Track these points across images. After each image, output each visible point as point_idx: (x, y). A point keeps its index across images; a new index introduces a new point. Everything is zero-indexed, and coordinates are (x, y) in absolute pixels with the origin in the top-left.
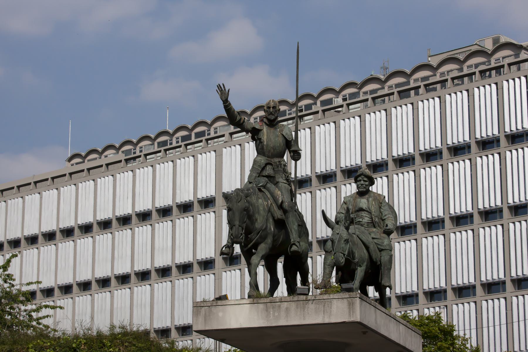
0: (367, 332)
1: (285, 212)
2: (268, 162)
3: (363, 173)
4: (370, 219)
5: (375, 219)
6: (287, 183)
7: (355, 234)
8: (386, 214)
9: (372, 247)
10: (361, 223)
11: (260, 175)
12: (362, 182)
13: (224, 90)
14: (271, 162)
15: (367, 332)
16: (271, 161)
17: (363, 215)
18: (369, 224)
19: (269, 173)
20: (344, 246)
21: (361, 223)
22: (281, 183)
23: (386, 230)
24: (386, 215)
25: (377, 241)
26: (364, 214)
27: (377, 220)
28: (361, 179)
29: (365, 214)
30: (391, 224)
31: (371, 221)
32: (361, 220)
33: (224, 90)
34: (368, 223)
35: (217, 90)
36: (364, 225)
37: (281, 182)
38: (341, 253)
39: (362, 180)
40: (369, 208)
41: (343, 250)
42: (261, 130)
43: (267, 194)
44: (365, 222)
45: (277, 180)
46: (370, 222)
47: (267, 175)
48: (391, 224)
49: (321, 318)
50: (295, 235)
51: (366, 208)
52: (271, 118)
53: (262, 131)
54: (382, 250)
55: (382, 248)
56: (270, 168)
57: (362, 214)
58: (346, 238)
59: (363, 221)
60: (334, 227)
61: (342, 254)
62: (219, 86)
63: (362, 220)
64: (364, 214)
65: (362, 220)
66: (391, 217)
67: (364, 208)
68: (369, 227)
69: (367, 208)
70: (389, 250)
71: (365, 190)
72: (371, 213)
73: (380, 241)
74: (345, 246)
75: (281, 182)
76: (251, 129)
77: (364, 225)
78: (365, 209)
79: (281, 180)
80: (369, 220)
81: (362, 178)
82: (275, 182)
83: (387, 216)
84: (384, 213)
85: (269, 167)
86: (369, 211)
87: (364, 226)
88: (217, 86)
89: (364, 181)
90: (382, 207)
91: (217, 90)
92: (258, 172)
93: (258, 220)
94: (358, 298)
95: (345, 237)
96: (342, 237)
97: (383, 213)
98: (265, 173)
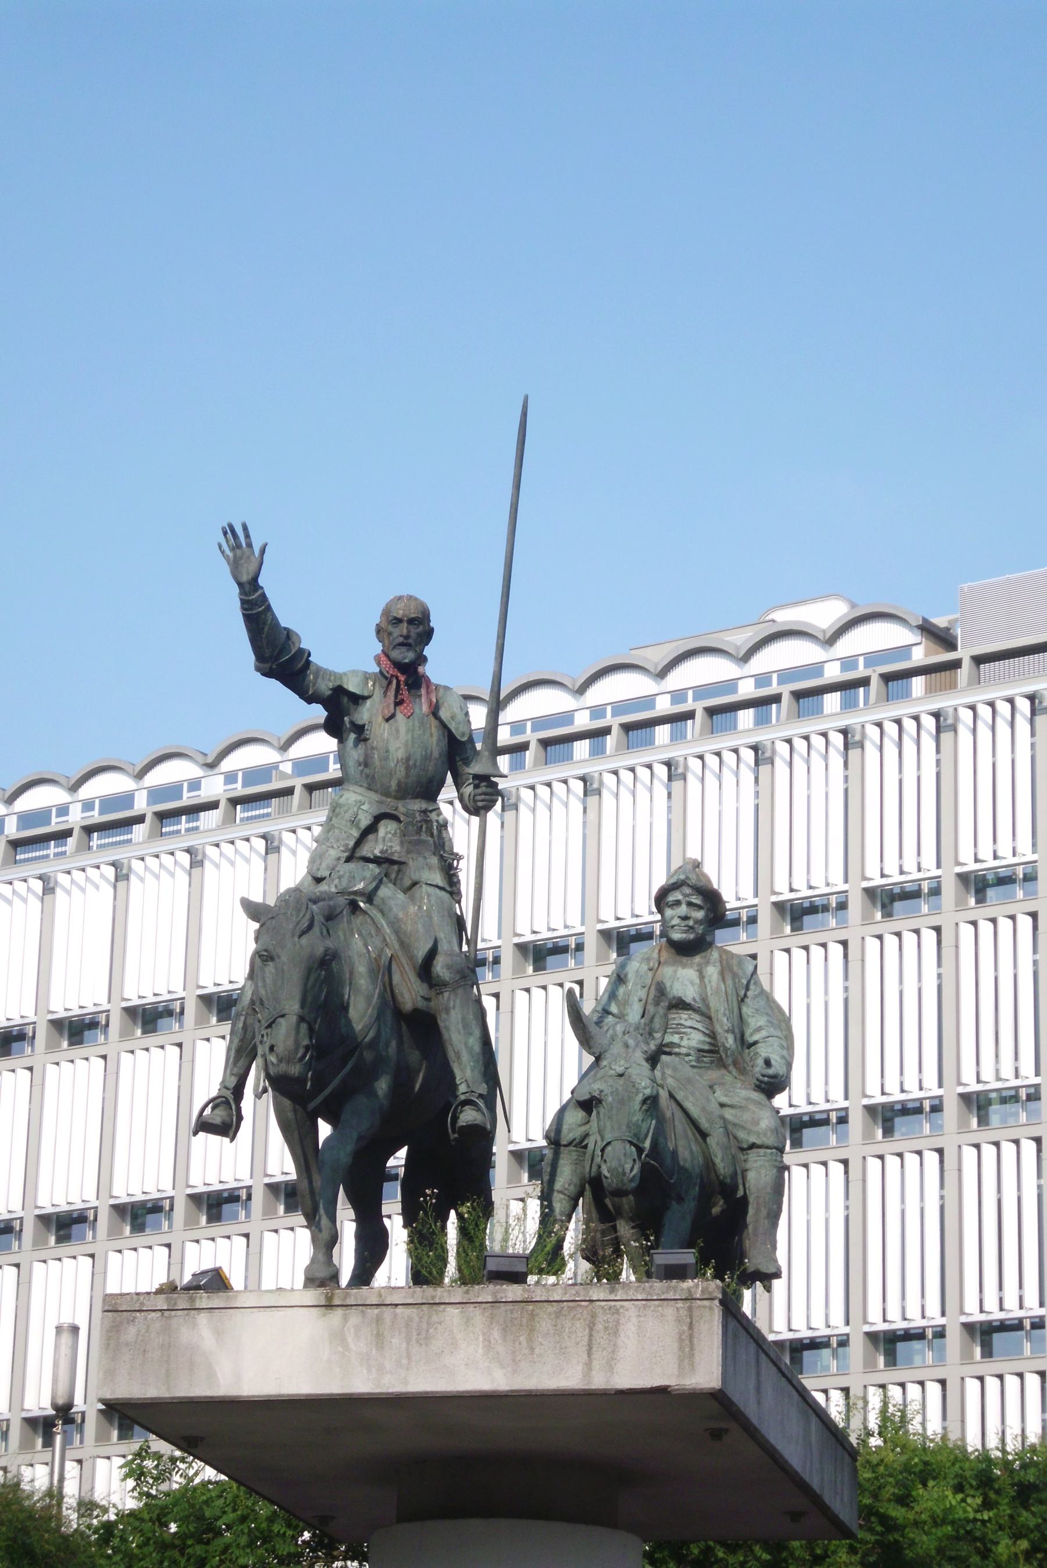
4: (707, 1039)
17: (682, 1022)
19: (387, 850)
26: (684, 1018)
34: (700, 1050)
42: (365, 698)
44: (689, 1048)
46: (706, 1047)
62: (229, 531)
63: (682, 1038)
67: (688, 999)
68: (703, 1065)
72: (710, 1018)
75: (427, 884)
80: (704, 1042)
81: (685, 895)
86: (703, 1009)
91: (220, 546)
95: (645, 1088)
98: (374, 847)
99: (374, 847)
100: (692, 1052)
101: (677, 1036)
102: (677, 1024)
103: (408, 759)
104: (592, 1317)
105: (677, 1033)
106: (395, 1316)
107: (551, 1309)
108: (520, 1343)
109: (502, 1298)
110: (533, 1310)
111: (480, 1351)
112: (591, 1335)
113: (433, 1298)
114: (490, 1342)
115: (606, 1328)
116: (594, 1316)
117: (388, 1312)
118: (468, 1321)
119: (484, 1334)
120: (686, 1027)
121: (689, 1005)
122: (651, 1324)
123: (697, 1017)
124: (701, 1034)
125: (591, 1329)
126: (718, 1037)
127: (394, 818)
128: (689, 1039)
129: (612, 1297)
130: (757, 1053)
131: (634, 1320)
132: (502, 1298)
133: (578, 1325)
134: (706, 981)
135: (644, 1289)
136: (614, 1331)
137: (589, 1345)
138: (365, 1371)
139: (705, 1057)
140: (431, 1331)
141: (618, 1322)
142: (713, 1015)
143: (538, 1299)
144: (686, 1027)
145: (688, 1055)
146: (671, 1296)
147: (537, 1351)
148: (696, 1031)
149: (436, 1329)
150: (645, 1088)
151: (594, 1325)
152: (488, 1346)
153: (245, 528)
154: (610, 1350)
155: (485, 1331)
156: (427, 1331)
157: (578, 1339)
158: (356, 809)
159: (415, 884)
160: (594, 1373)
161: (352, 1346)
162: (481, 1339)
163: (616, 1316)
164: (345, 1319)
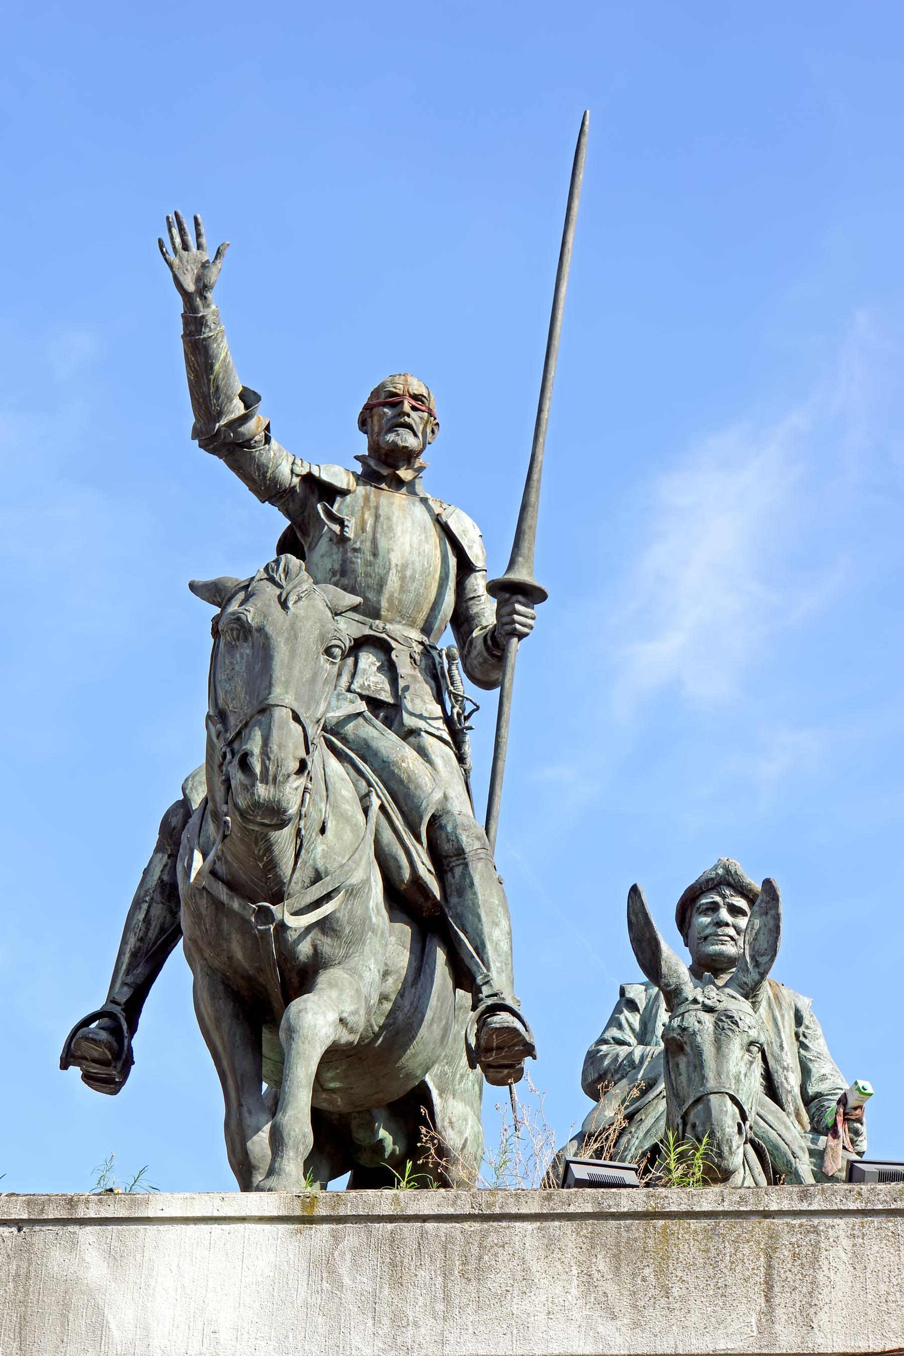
2: (368, 632)
3: (727, 871)
12: (724, 914)
14: (384, 636)
16: (384, 631)
20: (743, 1072)
35: (160, 242)
39: (721, 903)
42: (344, 493)
43: (361, 767)
50: (499, 973)
58: (753, 1034)
74: (746, 1075)
81: (724, 897)
89: (735, 911)
91: (160, 242)
103: (404, 567)
104: (771, 1237)
106: (423, 1234)
108: (644, 1280)
109: (610, 1206)
110: (665, 1228)
111: (574, 1291)
112: (769, 1267)
113: (490, 1205)
116: (773, 1236)
117: (409, 1230)
118: (551, 1245)
119: (580, 1264)
122: (876, 1248)
125: (769, 1258)
129: (804, 1206)
130: (823, 1106)
131: (846, 1242)
132: (610, 1206)
133: (746, 1251)
135: (860, 1194)
137: (767, 1283)
138: (370, 1322)
140: (486, 1258)
141: (816, 1246)
143: (674, 1208)
147: (675, 1291)
149: (496, 1255)
151: (775, 1250)
152: (589, 1282)
154: (804, 1290)
155: (581, 1258)
156: (480, 1258)
160: (778, 1327)
161: (347, 1280)
162: (575, 1272)
164: (336, 1239)
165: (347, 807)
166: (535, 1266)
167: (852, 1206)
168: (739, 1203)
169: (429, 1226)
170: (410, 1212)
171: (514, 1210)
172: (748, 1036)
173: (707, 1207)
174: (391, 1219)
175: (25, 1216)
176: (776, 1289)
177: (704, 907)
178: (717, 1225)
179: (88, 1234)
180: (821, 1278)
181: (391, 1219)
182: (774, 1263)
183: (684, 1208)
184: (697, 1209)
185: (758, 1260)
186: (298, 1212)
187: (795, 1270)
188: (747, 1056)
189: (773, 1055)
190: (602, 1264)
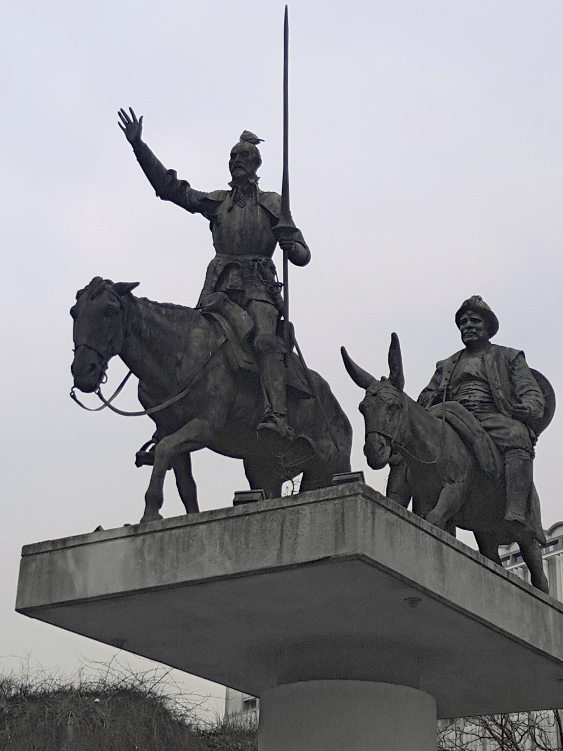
0: (419, 600)
1: (258, 356)
2: (230, 262)
4: (486, 395)
5: (498, 393)
6: (272, 303)
7: (441, 418)
8: (522, 384)
9: (480, 442)
10: (468, 404)
11: (215, 289)
12: (469, 323)
13: (132, 121)
15: (419, 600)
17: (471, 387)
18: (485, 404)
19: (234, 285)
20: (388, 419)
21: (468, 404)
22: (257, 302)
23: (517, 410)
24: (523, 387)
25: (497, 433)
26: (472, 385)
27: (501, 394)
28: (466, 317)
29: (477, 385)
30: (533, 402)
31: (490, 398)
32: (466, 397)
33: (132, 121)
34: (481, 402)
36: (474, 408)
37: (256, 300)
38: (379, 433)
40: (483, 373)
41: (384, 429)
44: (475, 401)
45: (248, 297)
46: (486, 400)
47: (229, 288)
48: (533, 402)
49: (275, 553)
51: (477, 373)
52: (238, 174)
53: (222, 205)
54: (507, 449)
55: (506, 444)
56: (235, 275)
57: (469, 386)
58: (391, 402)
59: (472, 399)
60: (370, 384)
61: (382, 437)
62: (122, 113)
63: (470, 397)
64: (473, 386)
65: (470, 397)
66: (537, 391)
67: (474, 374)
68: (485, 410)
69: (479, 373)
70: (522, 448)
71: (476, 338)
72: (488, 383)
73: (502, 431)
74: (390, 420)
75: (256, 300)
76: (200, 203)
77: (474, 408)
78: (476, 375)
79: (255, 296)
80: (484, 397)
81: (469, 315)
82: (245, 301)
83: (526, 389)
84: (519, 382)
85: (233, 274)
86: (484, 378)
87: (473, 410)
88: (119, 113)
89: (473, 320)
90: (515, 372)
92: (211, 287)
93: (184, 365)
94: (360, 497)
95: (389, 400)
96: (381, 399)
97: (518, 383)
98: (227, 285)
99: (227, 285)
100: (476, 404)
101: (467, 396)
102: (467, 389)
103: (241, 230)
104: (283, 518)
105: (468, 394)
106: (171, 535)
107: (258, 517)
111: (218, 550)
112: (282, 530)
114: (223, 543)
115: (291, 524)
116: (284, 518)
119: (220, 539)
120: (472, 389)
121: (474, 376)
123: (480, 383)
124: (482, 393)
126: (493, 393)
127: (238, 267)
128: (474, 396)
129: (296, 503)
134: (486, 362)
136: (295, 525)
138: (153, 573)
139: (487, 406)
140: (190, 541)
141: (298, 519)
142: (489, 381)
144: (472, 389)
145: (474, 405)
146: (331, 496)
147: (250, 546)
148: (479, 391)
150: (389, 400)
153: (130, 109)
154: (293, 538)
156: (189, 542)
157: (275, 534)
158: (215, 265)
159: (250, 301)
161: (147, 558)
163: (298, 515)
165: (194, 350)
166: (206, 542)
167: (312, 500)
168: (273, 505)
169: (173, 531)
170: (167, 527)
171: (200, 521)
172: (388, 404)
173: (263, 509)
174: (160, 531)
175: (51, 549)
176: (284, 539)
177: (462, 322)
178: (266, 515)
179: (69, 552)
180: (300, 532)
181: (160, 531)
182: (284, 528)
183: (255, 510)
184: (260, 510)
185: (278, 528)
186: (133, 533)
187: (291, 530)
188: (390, 412)
189: (492, 384)
190: (227, 538)
